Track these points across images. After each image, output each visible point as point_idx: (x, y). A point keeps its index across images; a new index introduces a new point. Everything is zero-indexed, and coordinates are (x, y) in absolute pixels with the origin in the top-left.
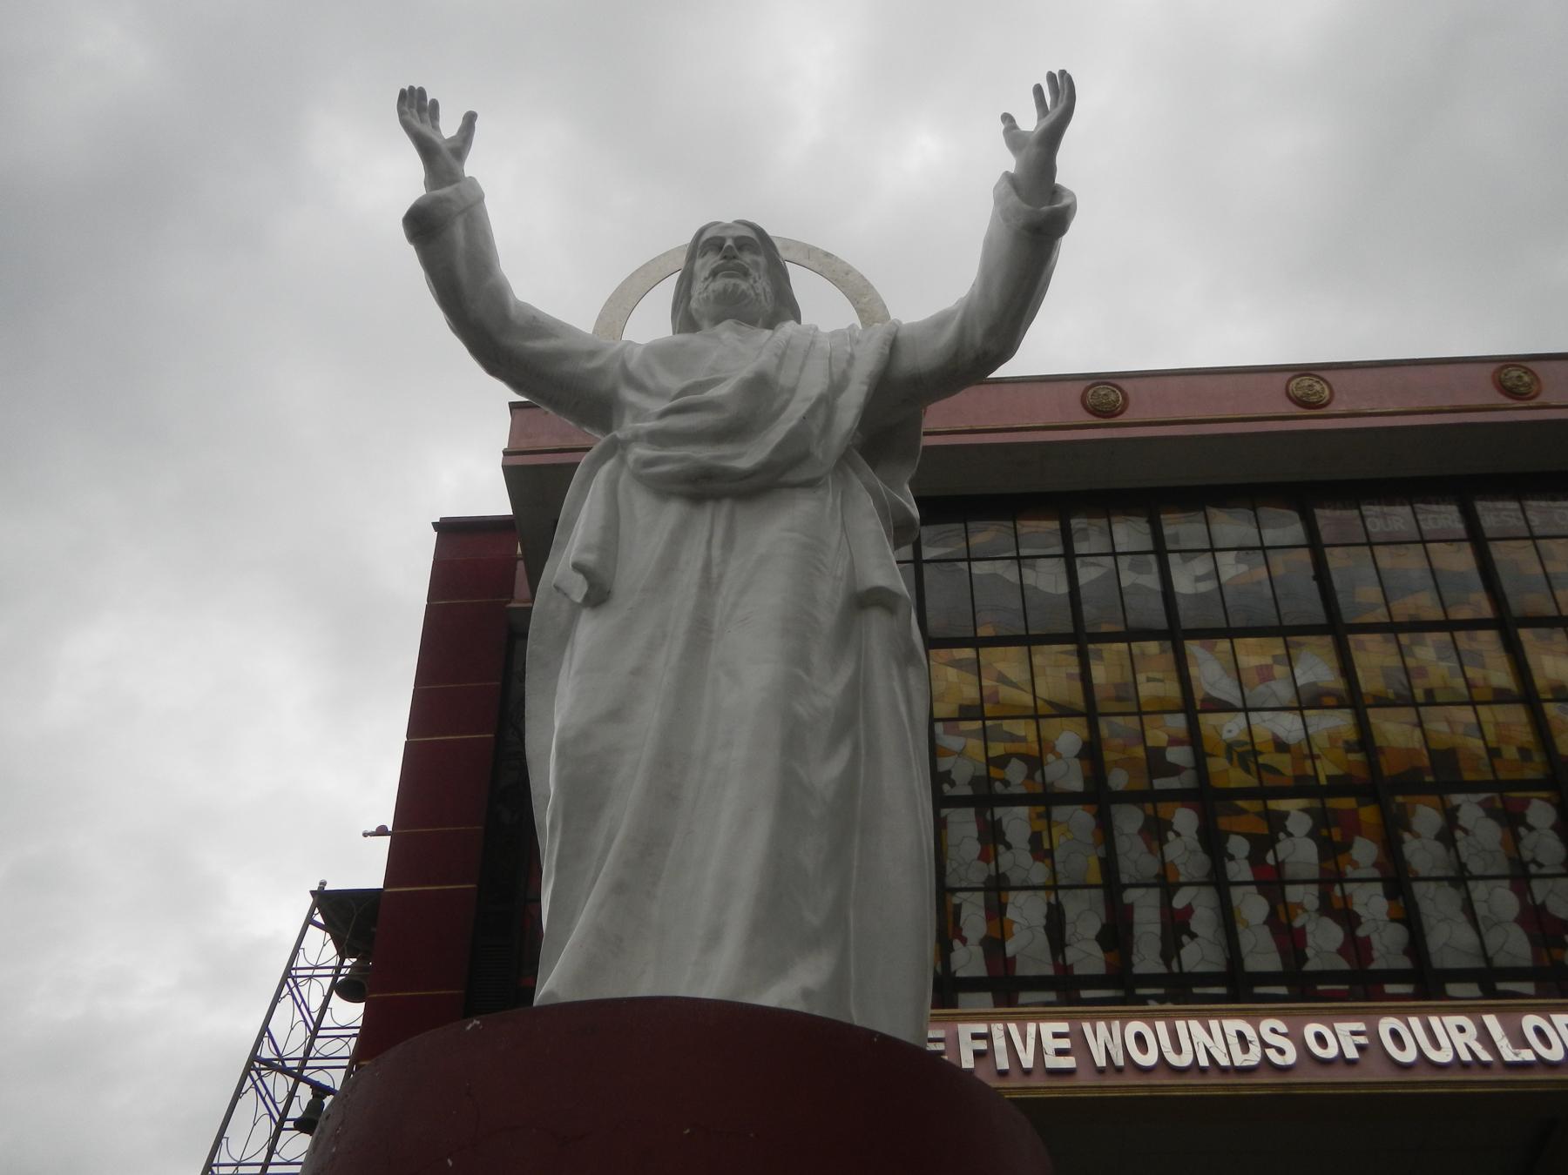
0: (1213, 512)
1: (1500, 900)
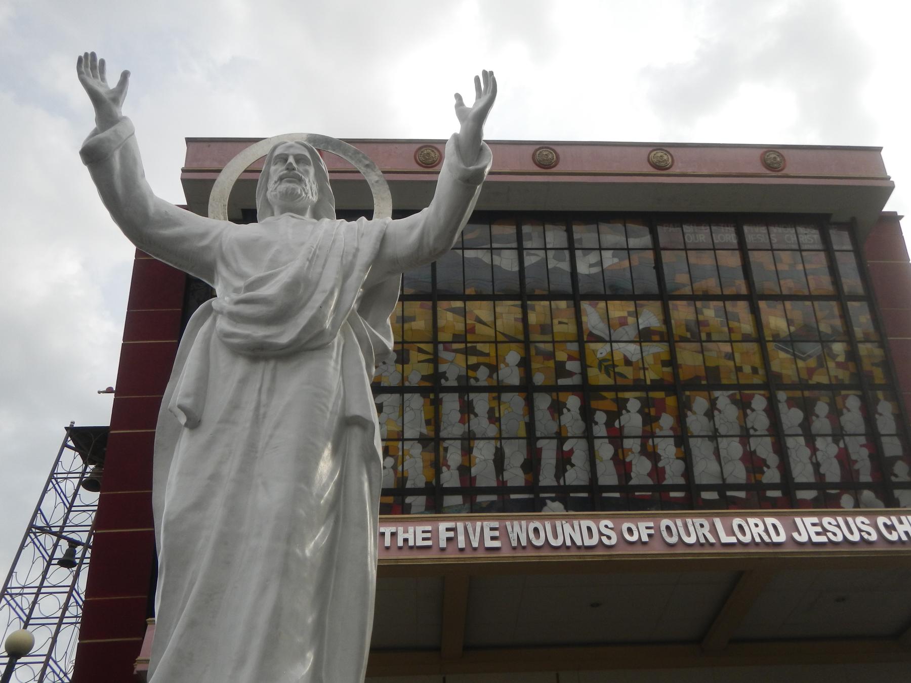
0: (604, 227)
1: (733, 448)
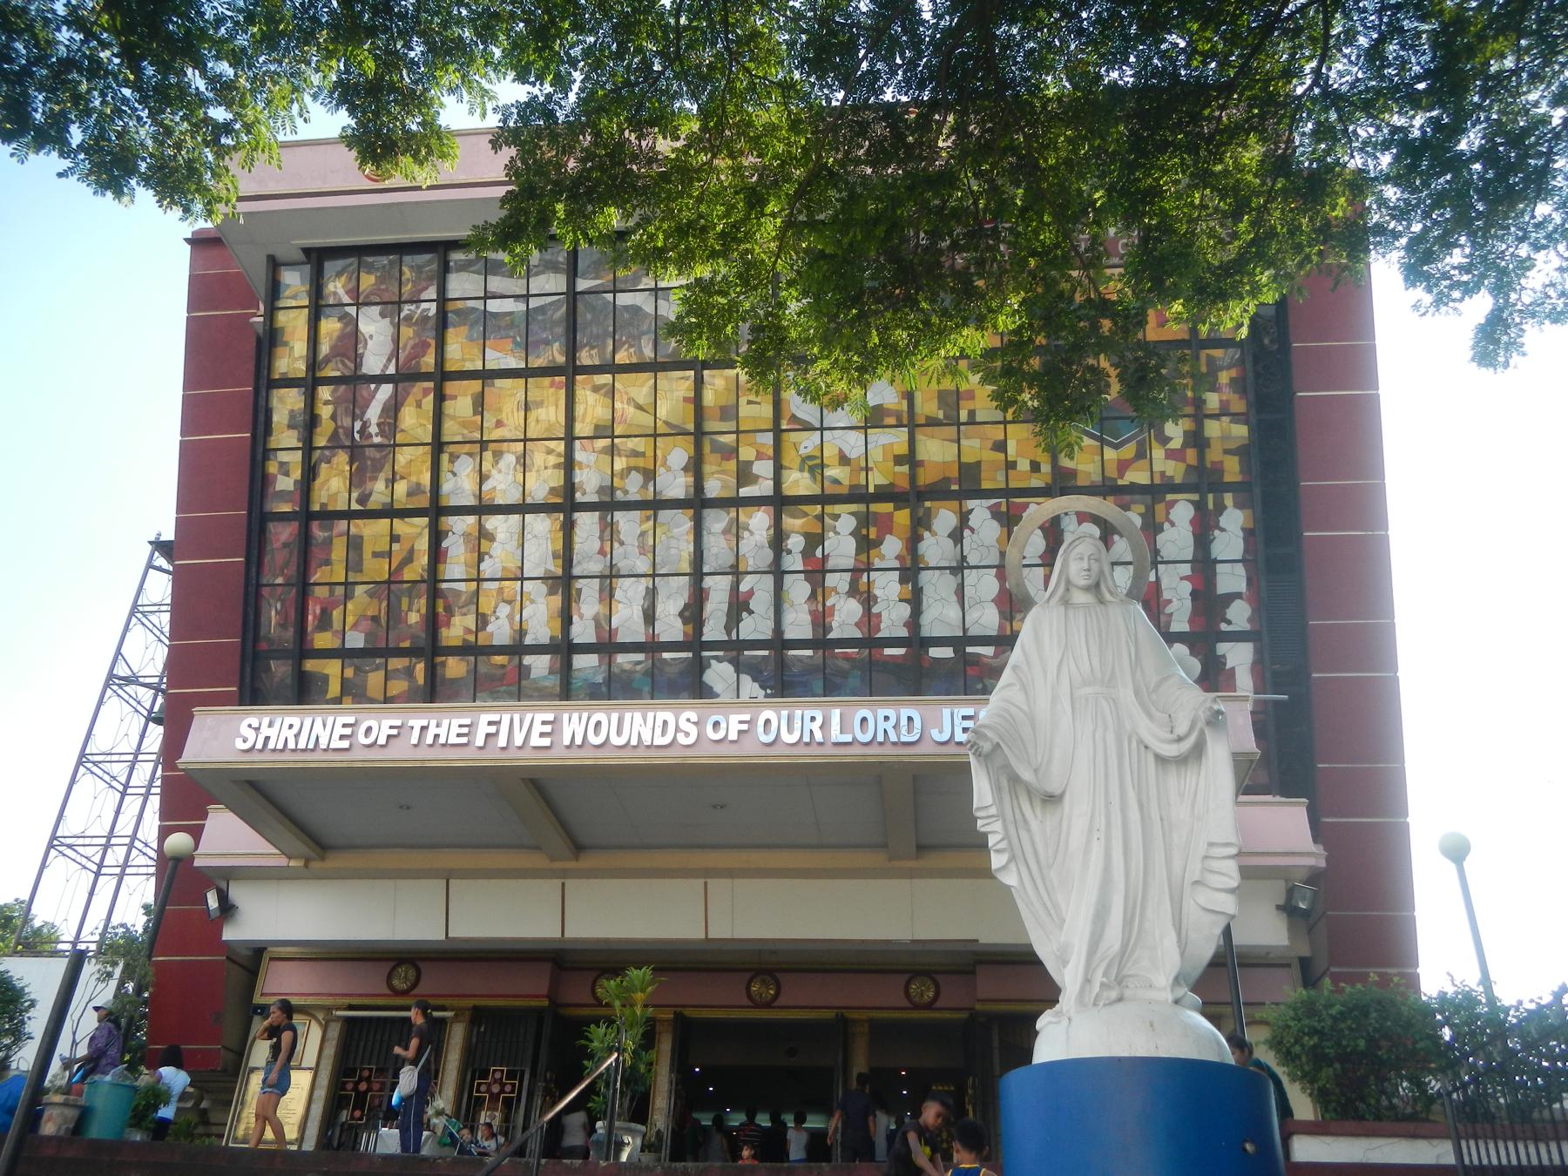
1: (984, 585)
